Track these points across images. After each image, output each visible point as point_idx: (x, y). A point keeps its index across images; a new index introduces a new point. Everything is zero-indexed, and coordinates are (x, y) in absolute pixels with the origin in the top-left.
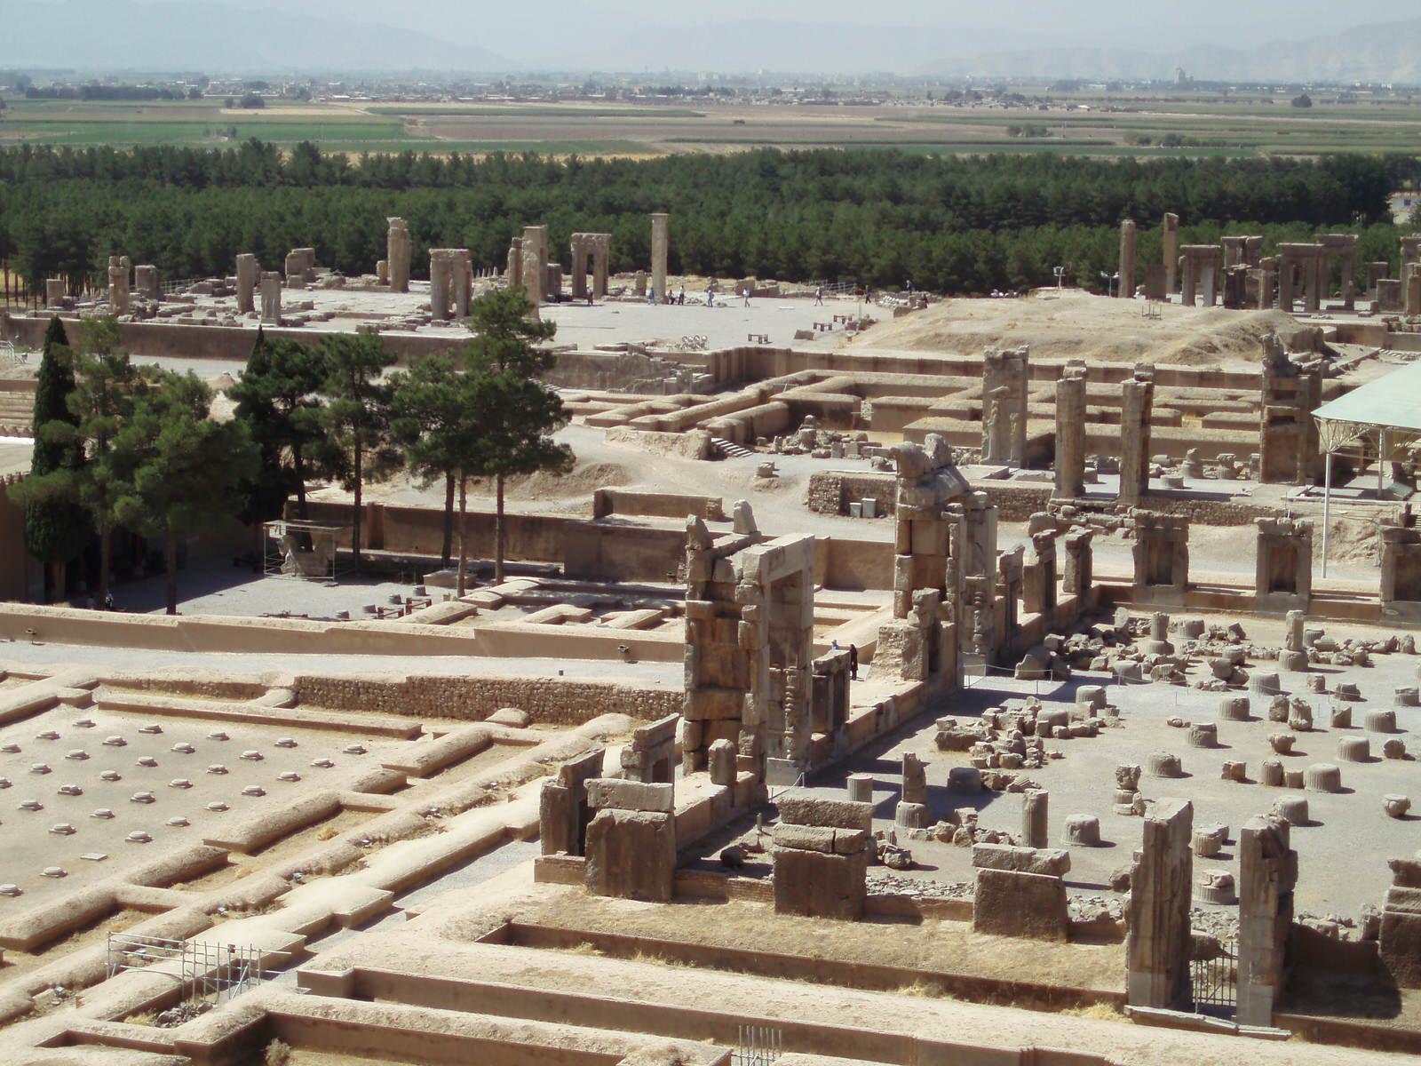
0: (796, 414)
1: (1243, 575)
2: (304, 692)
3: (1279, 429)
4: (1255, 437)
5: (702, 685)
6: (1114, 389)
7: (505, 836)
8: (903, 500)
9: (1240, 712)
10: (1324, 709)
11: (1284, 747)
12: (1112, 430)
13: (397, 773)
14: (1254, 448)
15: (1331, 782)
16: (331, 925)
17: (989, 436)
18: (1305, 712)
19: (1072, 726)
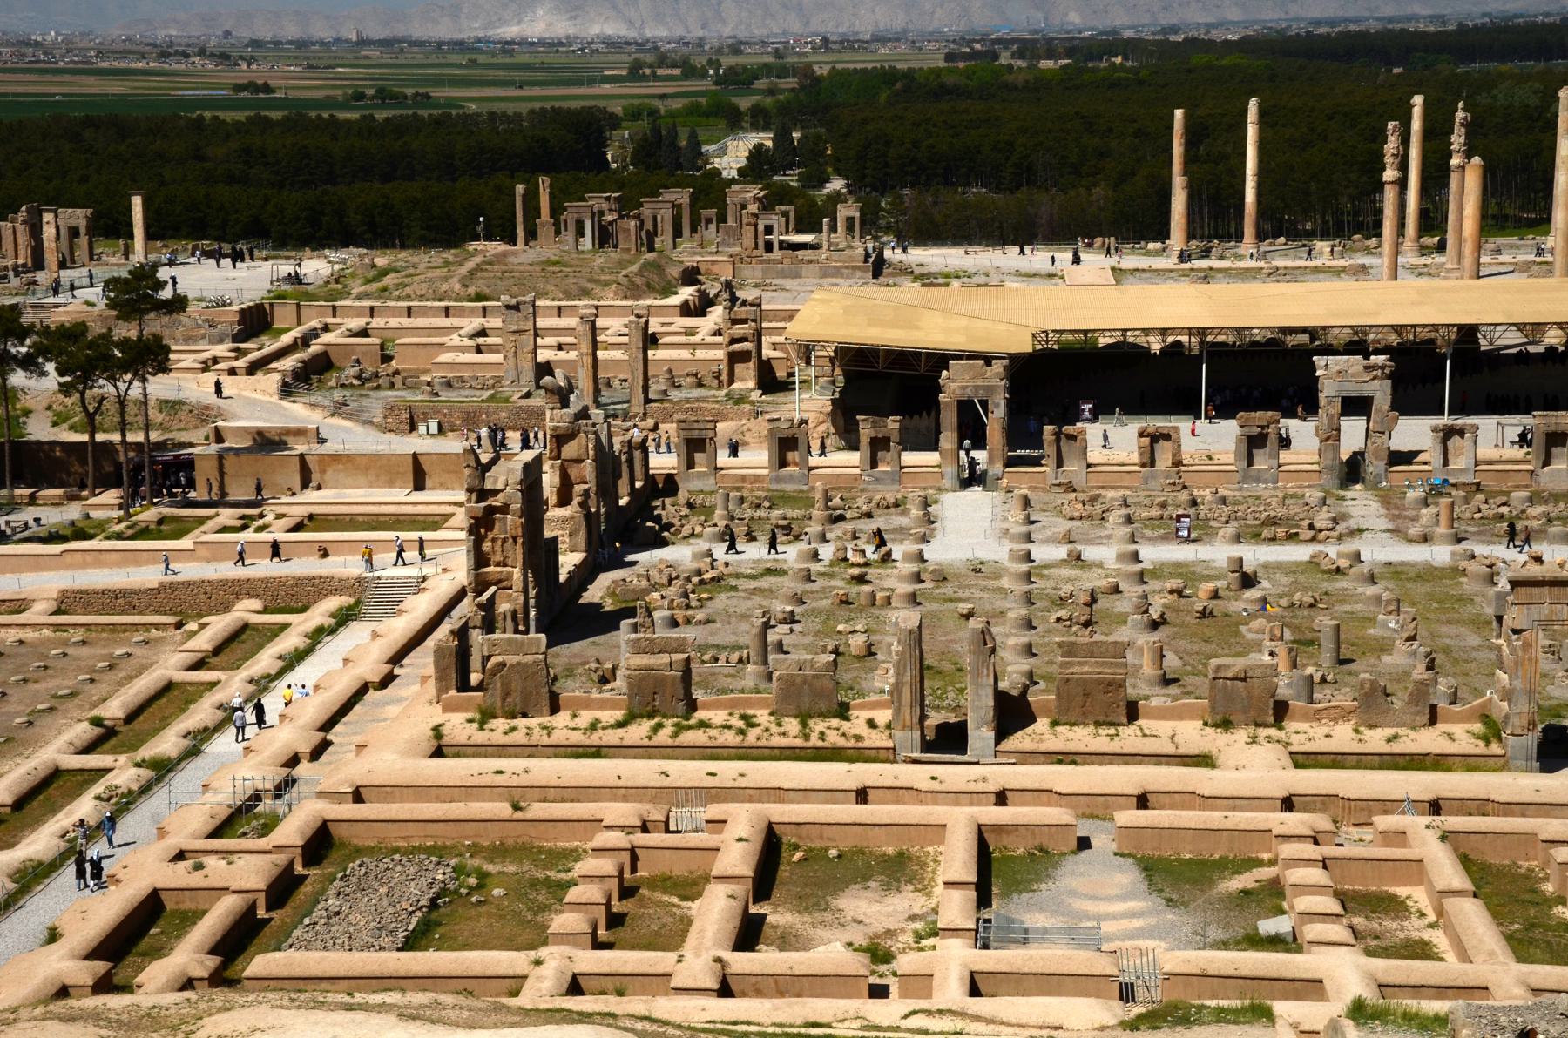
1: (757, 457)
3: (737, 347)
4: (720, 354)
8: (552, 419)
13: (200, 655)
17: (511, 361)
19: (707, 576)
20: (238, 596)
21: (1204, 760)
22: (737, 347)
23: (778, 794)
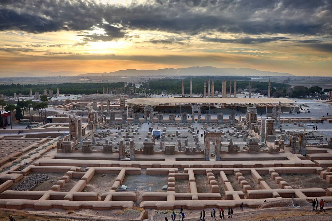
0: (74, 106)
2: (27, 136)
3: (121, 105)
5: (71, 131)
6: (106, 102)
7: (53, 148)
9: (122, 131)
10: (131, 130)
11: (128, 134)
12: (107, 106)
14: (119, 107)
15: (132, 137)
16: (36, 159)
18: (129, 130)
20: (48, 136)
21: (164, 160)
22: (121, 105)
23: (99, 165)
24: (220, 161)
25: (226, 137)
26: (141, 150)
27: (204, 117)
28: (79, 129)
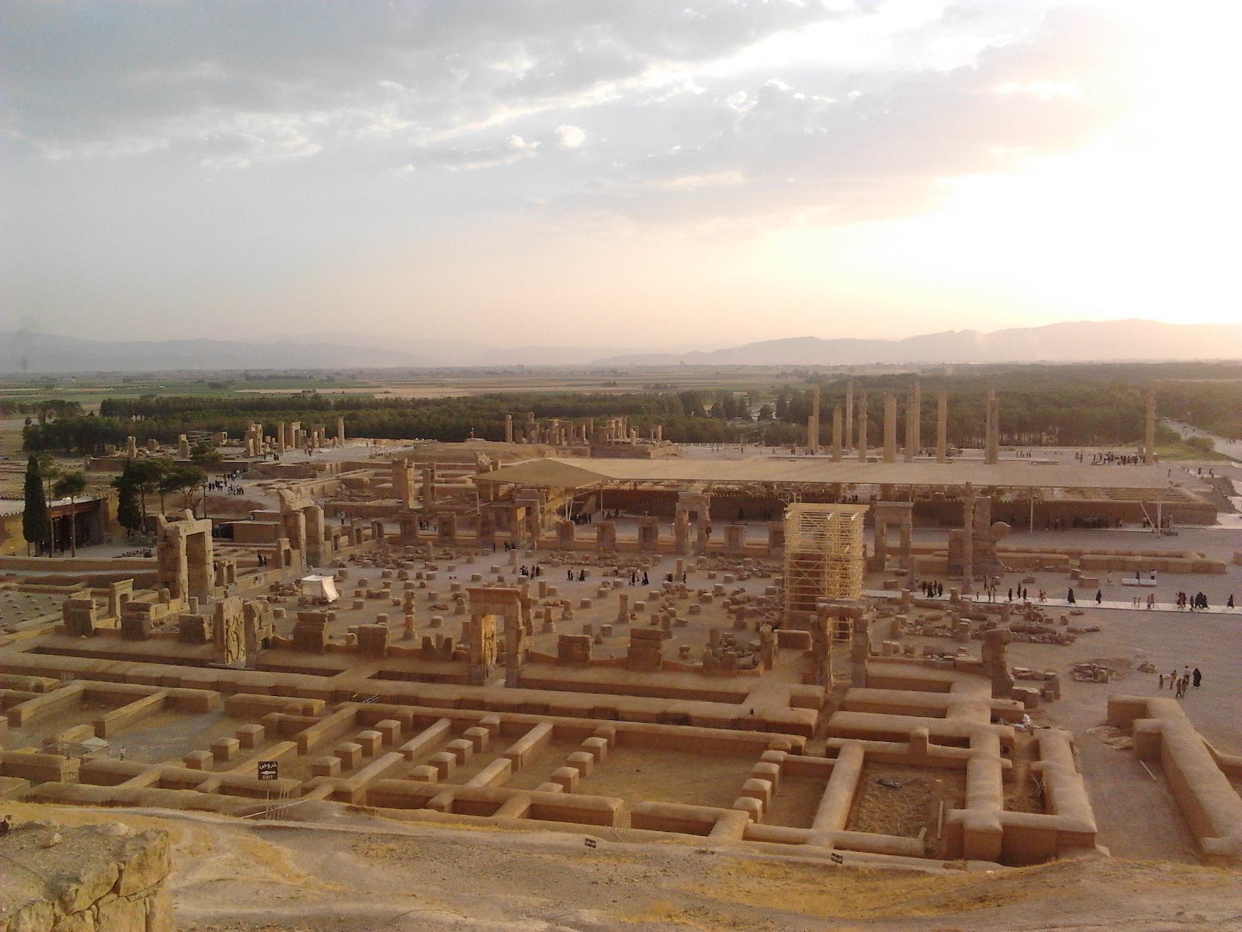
24: (518, 688)
25: (694, 610)
26: (349, 639)
27: (718, 537)
28: (196, 560)
